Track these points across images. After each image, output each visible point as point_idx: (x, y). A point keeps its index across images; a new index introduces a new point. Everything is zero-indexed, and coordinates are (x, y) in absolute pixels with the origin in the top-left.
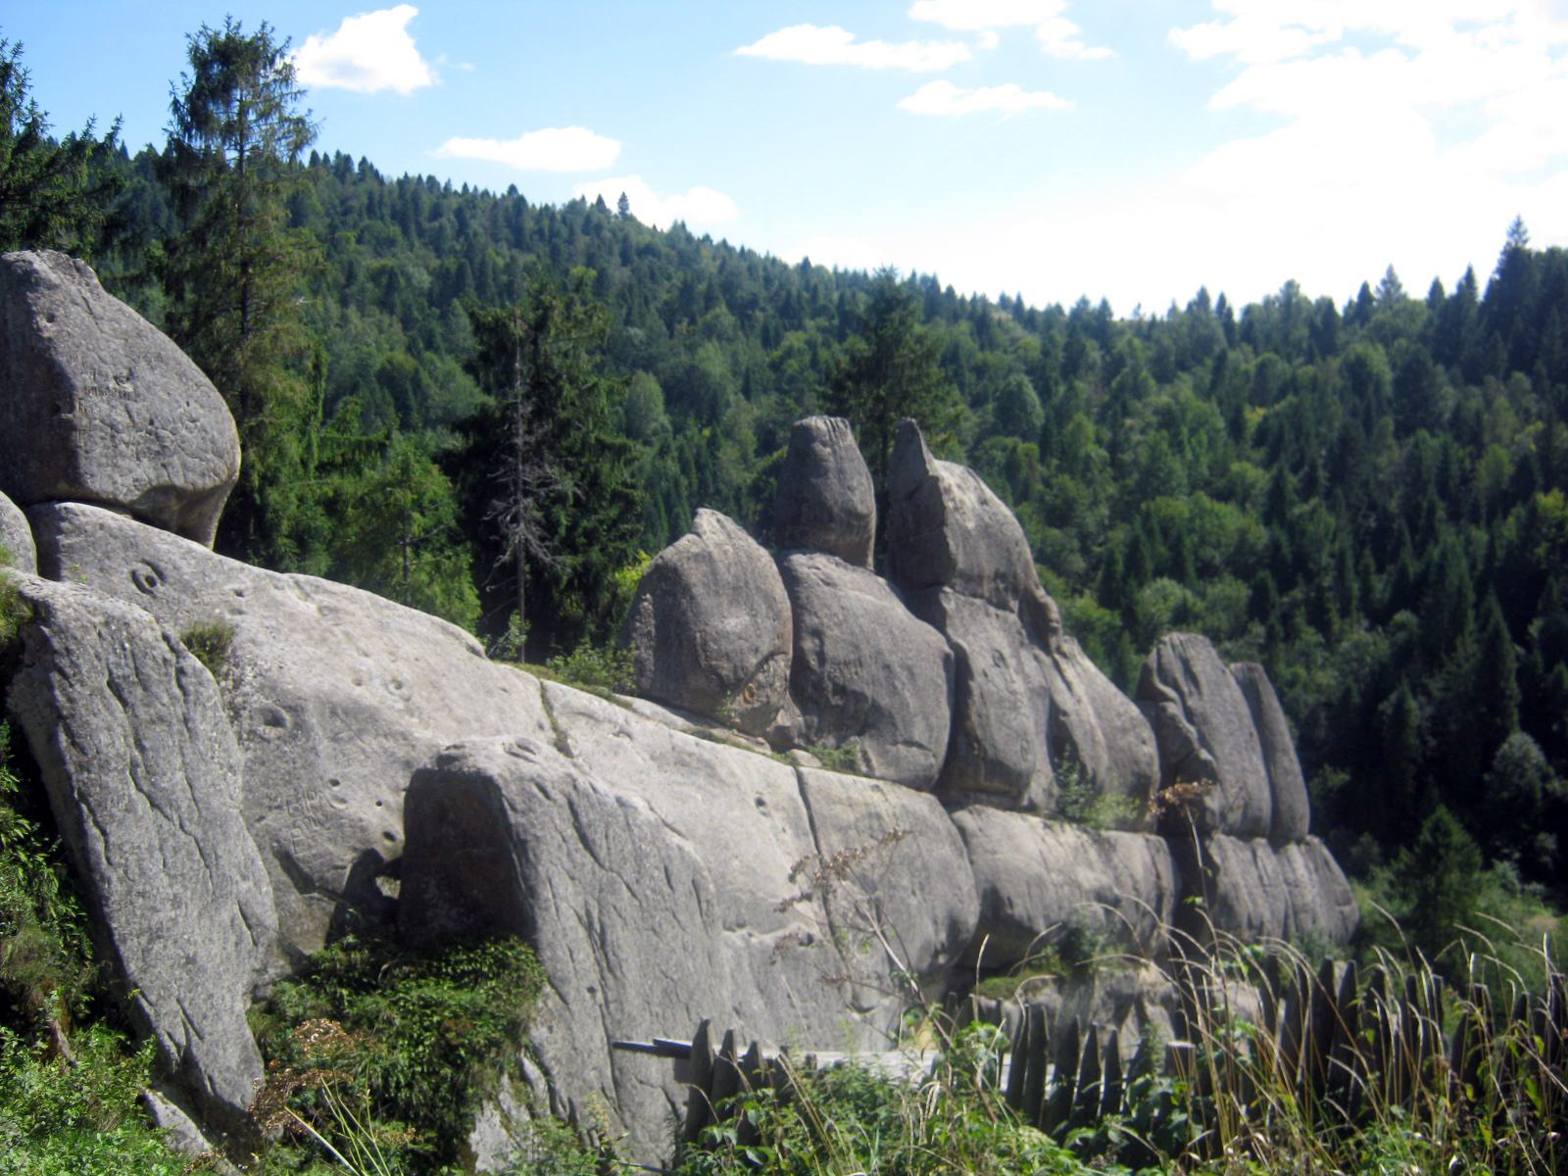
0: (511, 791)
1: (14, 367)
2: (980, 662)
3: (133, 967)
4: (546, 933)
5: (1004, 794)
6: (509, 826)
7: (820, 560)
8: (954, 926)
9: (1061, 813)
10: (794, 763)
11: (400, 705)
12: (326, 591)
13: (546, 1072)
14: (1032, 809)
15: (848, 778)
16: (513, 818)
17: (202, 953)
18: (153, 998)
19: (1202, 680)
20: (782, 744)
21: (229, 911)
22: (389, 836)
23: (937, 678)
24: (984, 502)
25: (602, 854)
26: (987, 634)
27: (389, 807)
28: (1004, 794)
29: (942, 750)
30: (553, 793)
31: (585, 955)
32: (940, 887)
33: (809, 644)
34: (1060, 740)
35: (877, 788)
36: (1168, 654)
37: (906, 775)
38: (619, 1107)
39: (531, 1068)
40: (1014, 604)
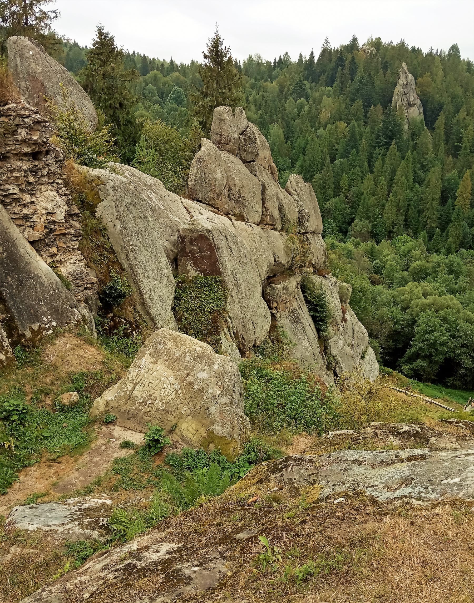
0: (214, 233)
1: (23, 84)
2: (267, 186)
3: (148, 301)
4: (226, 278)
5: (271, 225)
6: (215, 245)
7: (228, 154)
8: (270, 265)
9: (282, 230)
10: (231, 219)
11: (163, 208)
12: (128, 170)
13: (231, 319)
14: (276, 229)
15: (244, 223)
16: (216, 242)
17: (162, 295)
18: (154, 311)
19: (303, 188)
20: (227, 214)
21: (165, 281)
22: (172, 251)
23: (258, 192)
24: (259, 134)
25: (233, 250)
26: (266, 178)
27: (169, 242)
28: (271, 225)
29: (261, 212)
30: (223, 233)
31: (234, 283)
32: (267, 254)
33: (230, 182)
34: (281, 210)
35: (250, 226)
36: (293, 180)
37: (256, 221)
38: (244, 327)
39: (228, 318)
40: (267, 167)
